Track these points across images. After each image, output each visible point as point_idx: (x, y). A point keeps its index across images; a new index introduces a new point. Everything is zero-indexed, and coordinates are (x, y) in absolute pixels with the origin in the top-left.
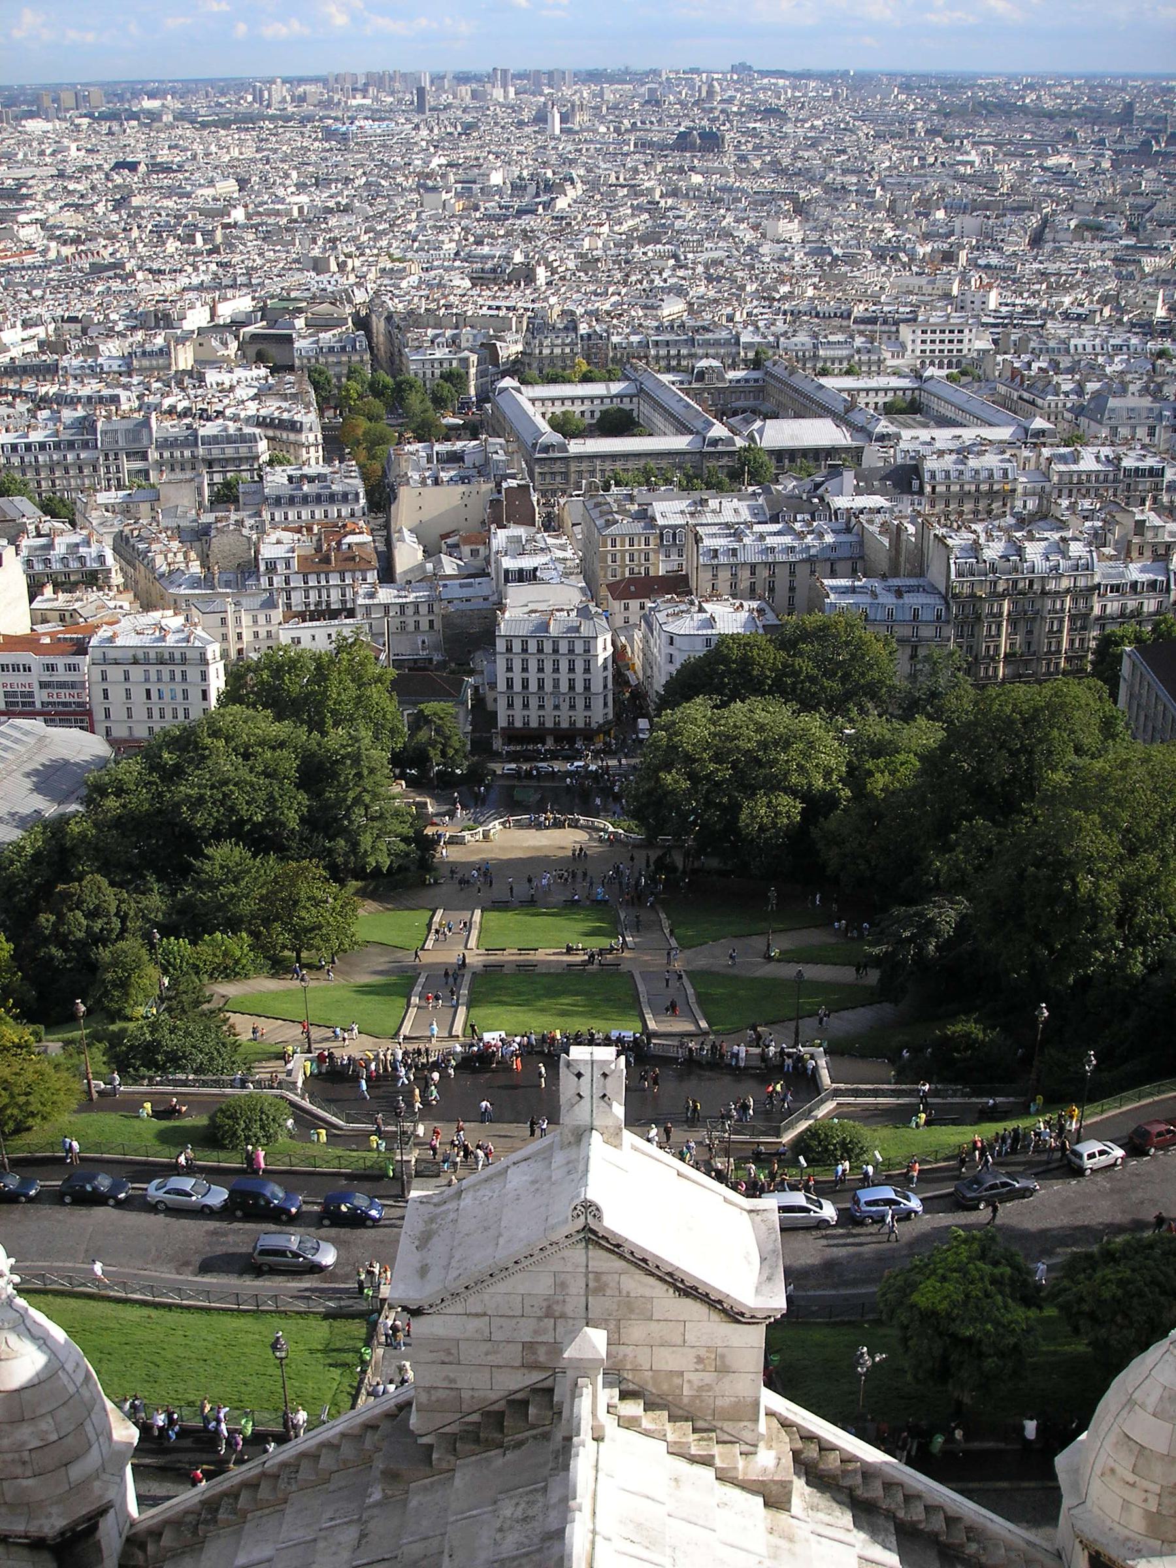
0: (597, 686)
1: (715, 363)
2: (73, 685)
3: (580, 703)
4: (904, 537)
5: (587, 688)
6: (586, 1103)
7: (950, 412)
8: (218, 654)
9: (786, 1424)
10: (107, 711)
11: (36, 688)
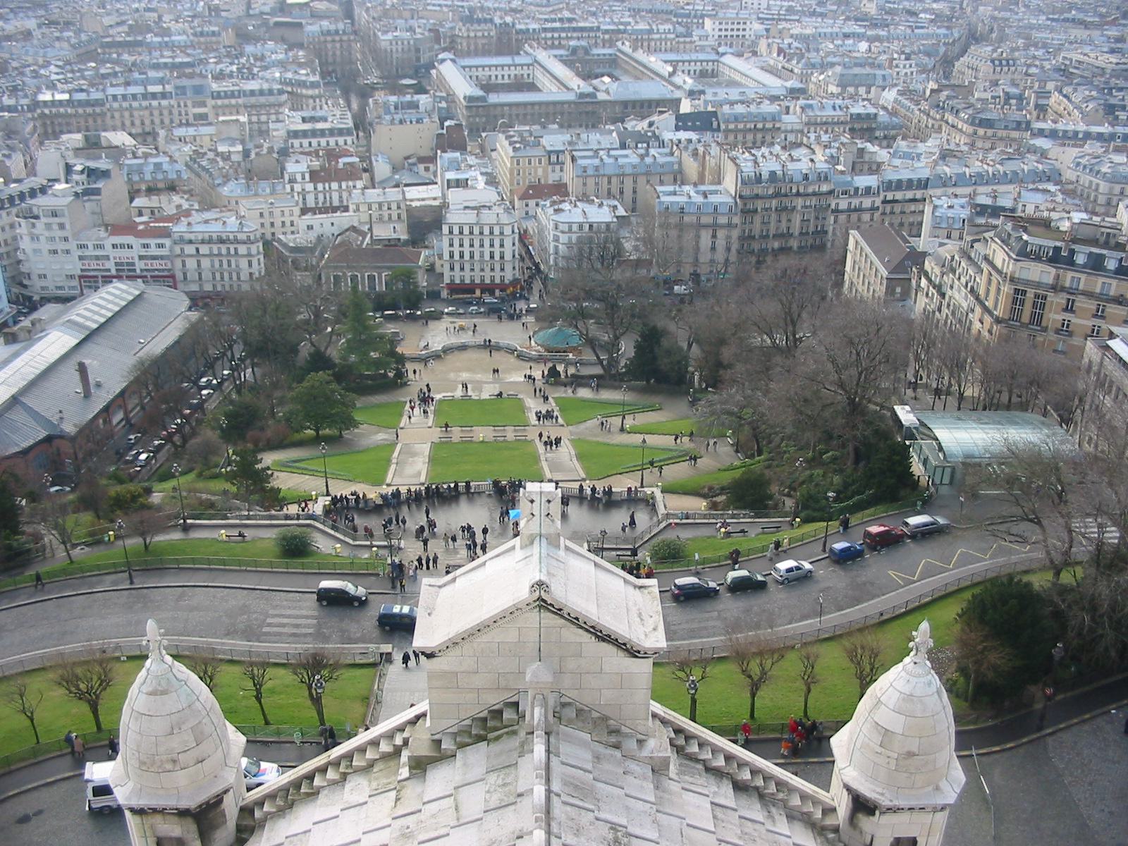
0: (508, 256)
1: (584, 43)
2: (162, 257)
3: (497, 267)
4: (707, 158)
5: (502, 257)
7: (738, 78)
8: (258, 236)
9: (664, 722)
10: (185, 274)
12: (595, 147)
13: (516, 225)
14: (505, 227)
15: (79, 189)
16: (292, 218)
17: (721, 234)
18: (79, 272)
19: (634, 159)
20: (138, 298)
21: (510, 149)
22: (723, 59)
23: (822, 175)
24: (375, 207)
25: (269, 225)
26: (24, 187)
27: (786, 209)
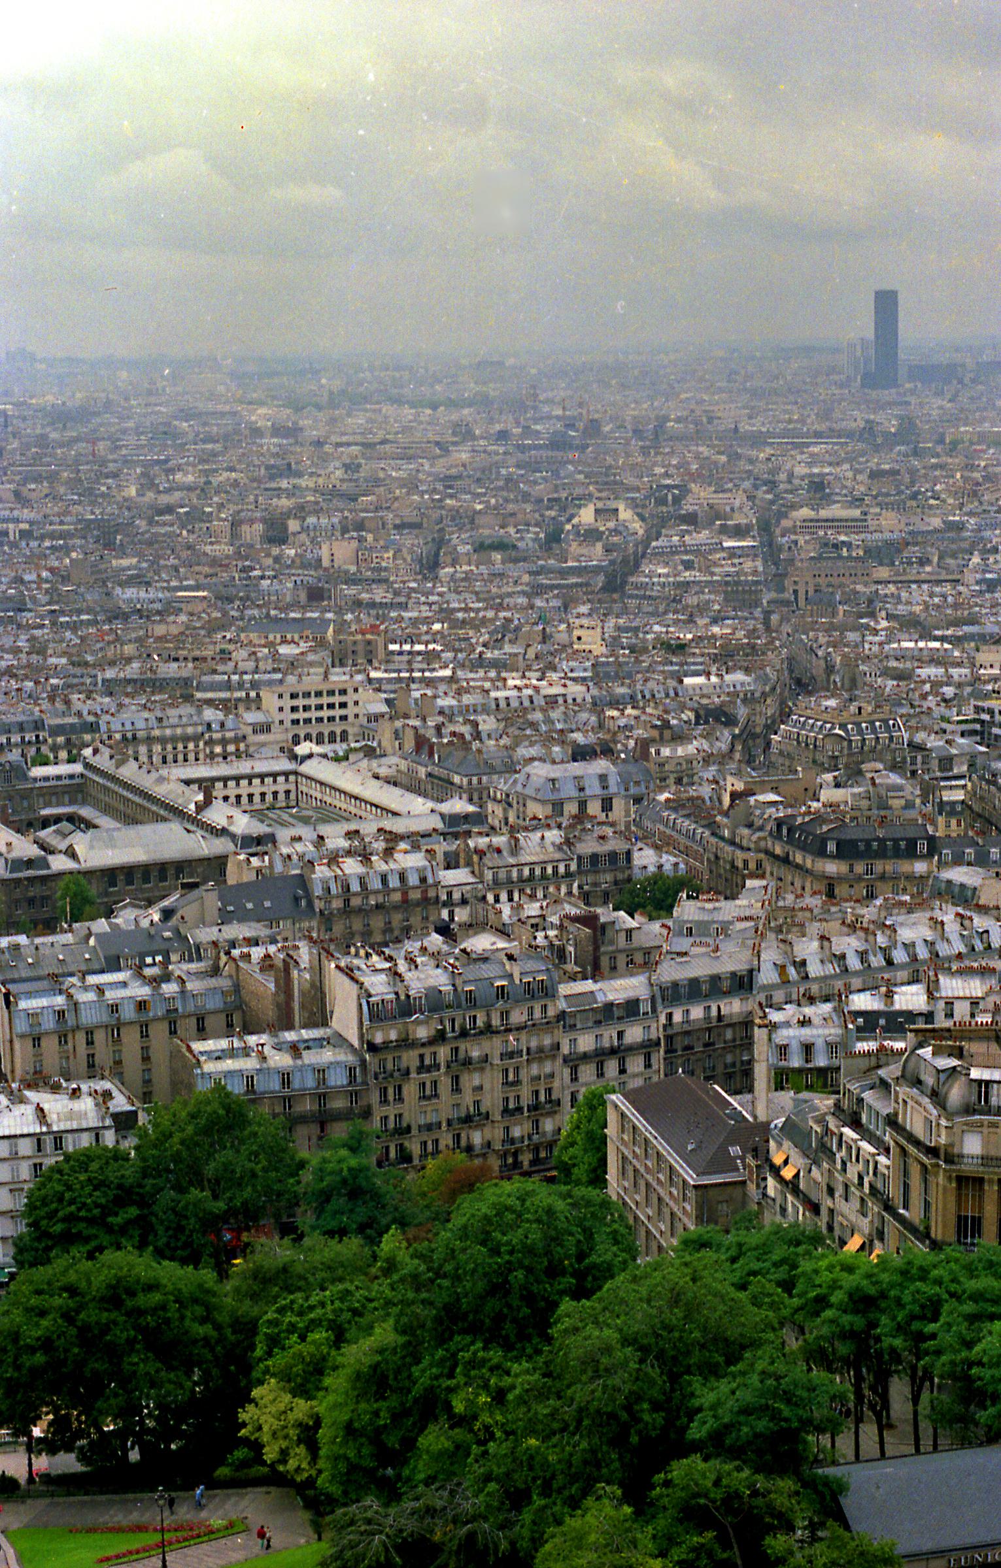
4: (295, 974)
7: (341, 803)
22: (307, 768)
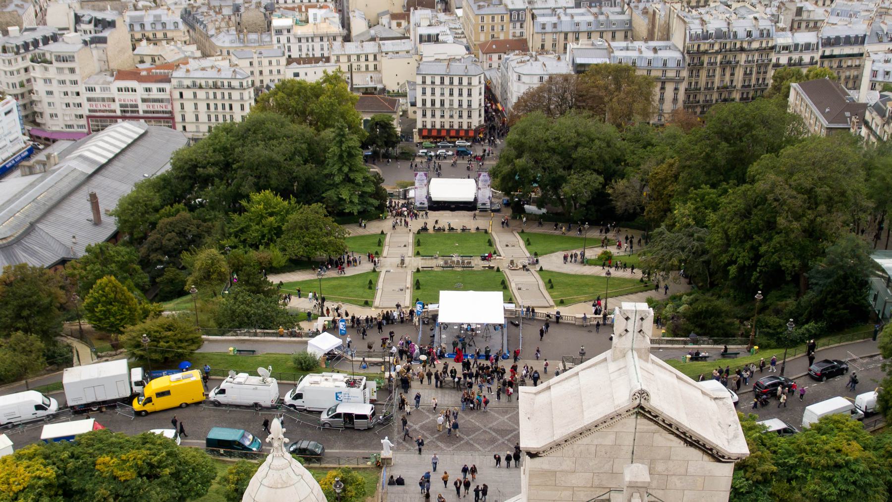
2: (161, 101)
6: (630, 334)
11: (139, 102)
12: (553, 5)
13: (482, 76)
14: (473, 78)
15: (87, 38)
16: (278, 68)
17: (670, 88)
18: (88, 113)
19: (591, 18)
20: (142, 136)
21: (475, 7)
23: (765, 32)
24: (353, 58)
25: (258, 73)
26: (38, 35)
27: (729, 62)
